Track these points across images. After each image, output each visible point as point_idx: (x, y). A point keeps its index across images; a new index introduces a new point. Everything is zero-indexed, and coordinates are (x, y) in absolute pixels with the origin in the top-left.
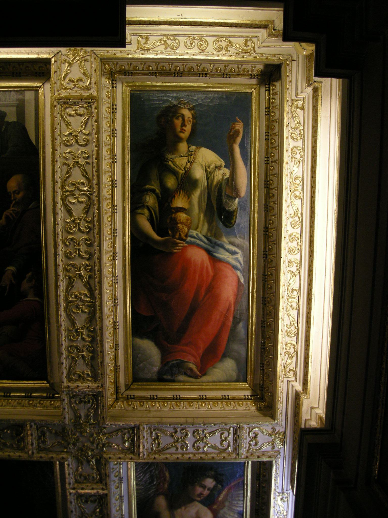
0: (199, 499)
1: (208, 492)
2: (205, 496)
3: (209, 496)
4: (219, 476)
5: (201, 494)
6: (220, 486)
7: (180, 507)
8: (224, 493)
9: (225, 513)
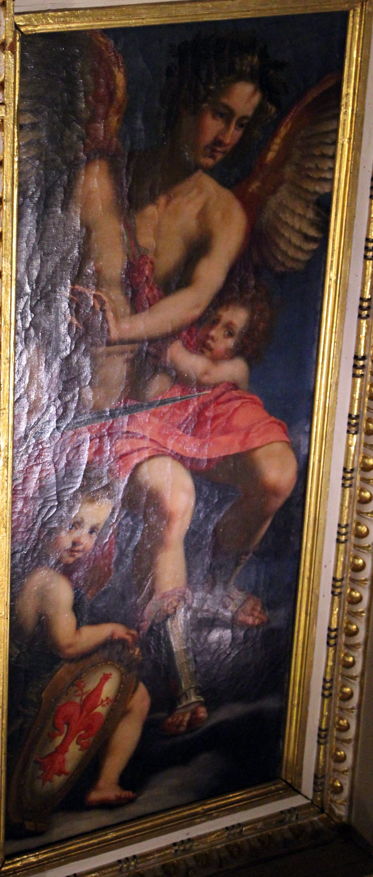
0: (210, 162)
1: (239, 133)
2: (228, 148)
3: (241, 144)
4: (272, 72)
5: (217, 142)
6: (272, 109)
7: (153, 199)
8: (283, 131)
9: (282, 206)
